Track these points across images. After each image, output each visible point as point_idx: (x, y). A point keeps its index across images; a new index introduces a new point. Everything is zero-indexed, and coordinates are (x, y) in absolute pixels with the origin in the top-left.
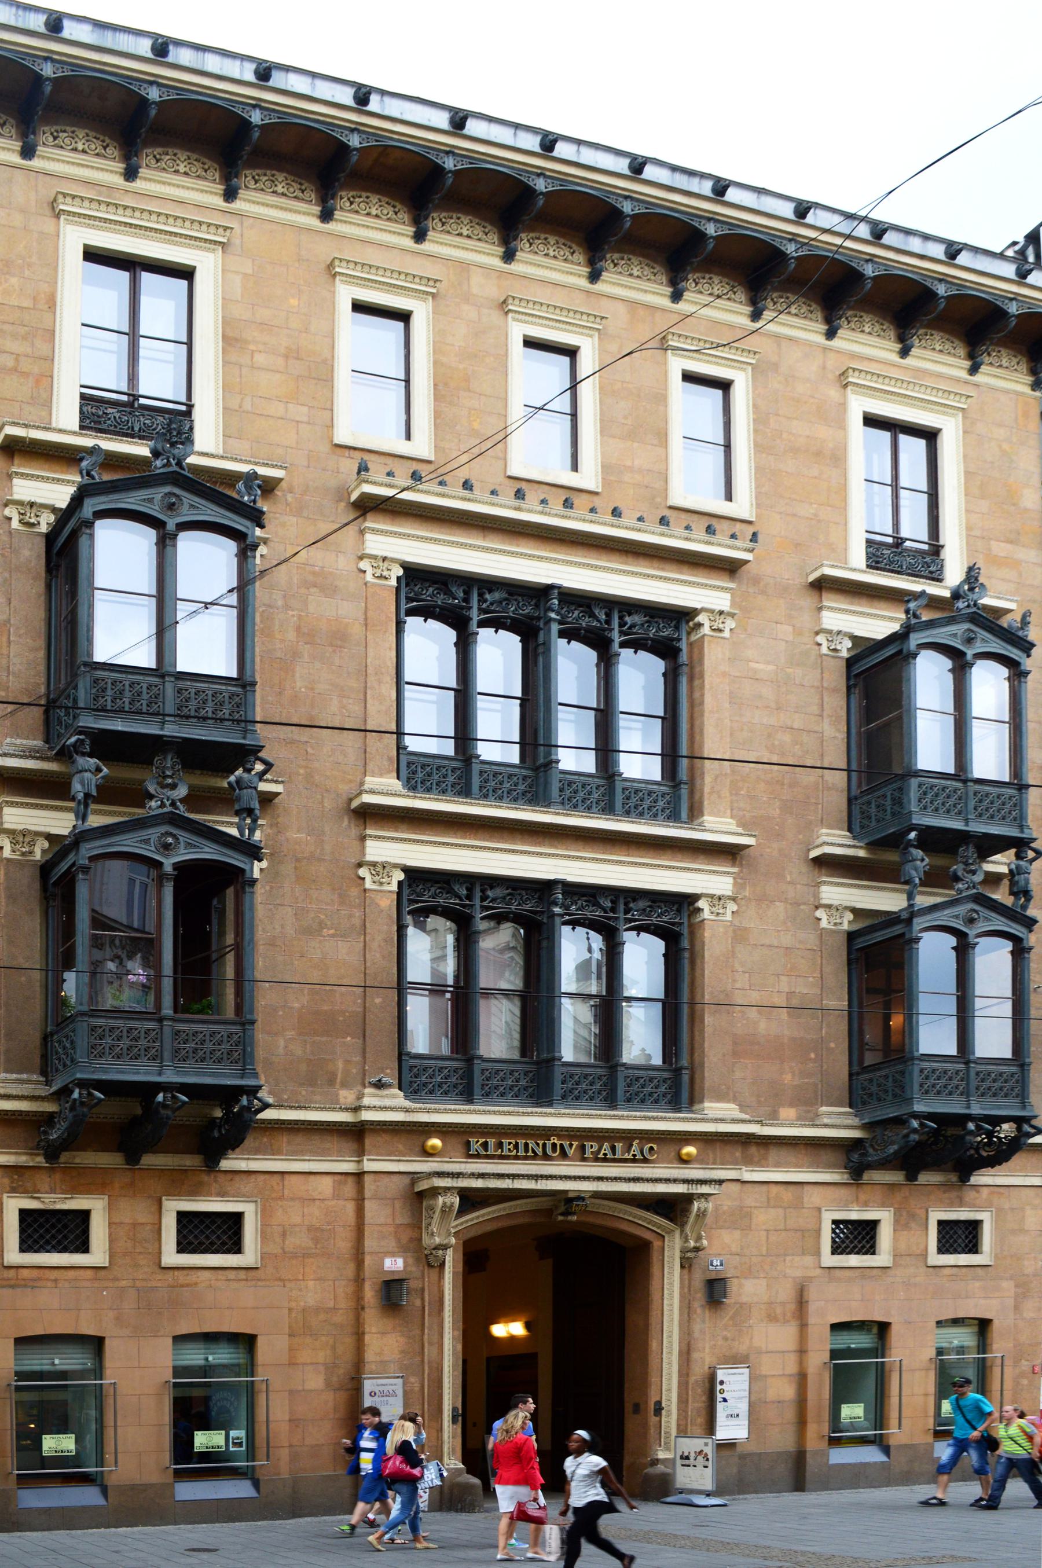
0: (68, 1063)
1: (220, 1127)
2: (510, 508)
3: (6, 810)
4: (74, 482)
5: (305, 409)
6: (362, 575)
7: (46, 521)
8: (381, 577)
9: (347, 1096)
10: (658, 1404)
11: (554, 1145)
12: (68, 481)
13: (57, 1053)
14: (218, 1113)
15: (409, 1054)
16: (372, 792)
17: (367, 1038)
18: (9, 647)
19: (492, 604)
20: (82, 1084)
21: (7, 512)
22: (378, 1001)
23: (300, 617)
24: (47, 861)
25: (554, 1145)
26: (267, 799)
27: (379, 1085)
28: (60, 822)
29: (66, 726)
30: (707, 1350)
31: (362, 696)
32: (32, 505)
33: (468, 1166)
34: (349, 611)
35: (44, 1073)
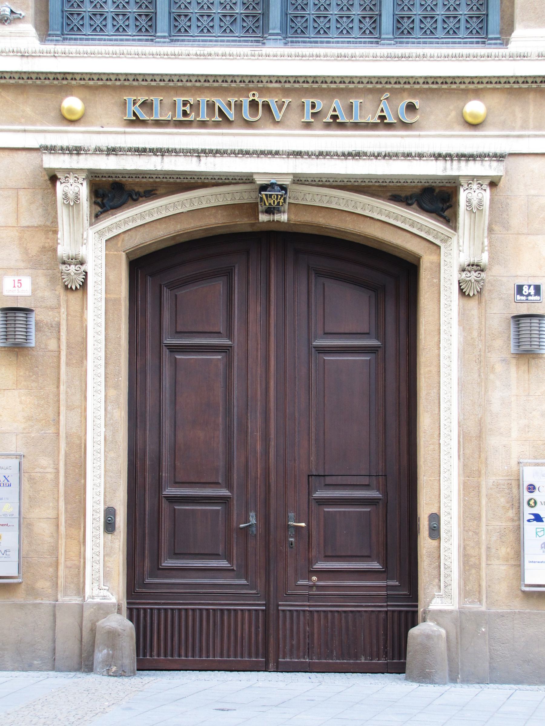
10: (435, 518)
11: (254, 104)
25: (254, 104)
30: (514, 434)
33: (128, 137)
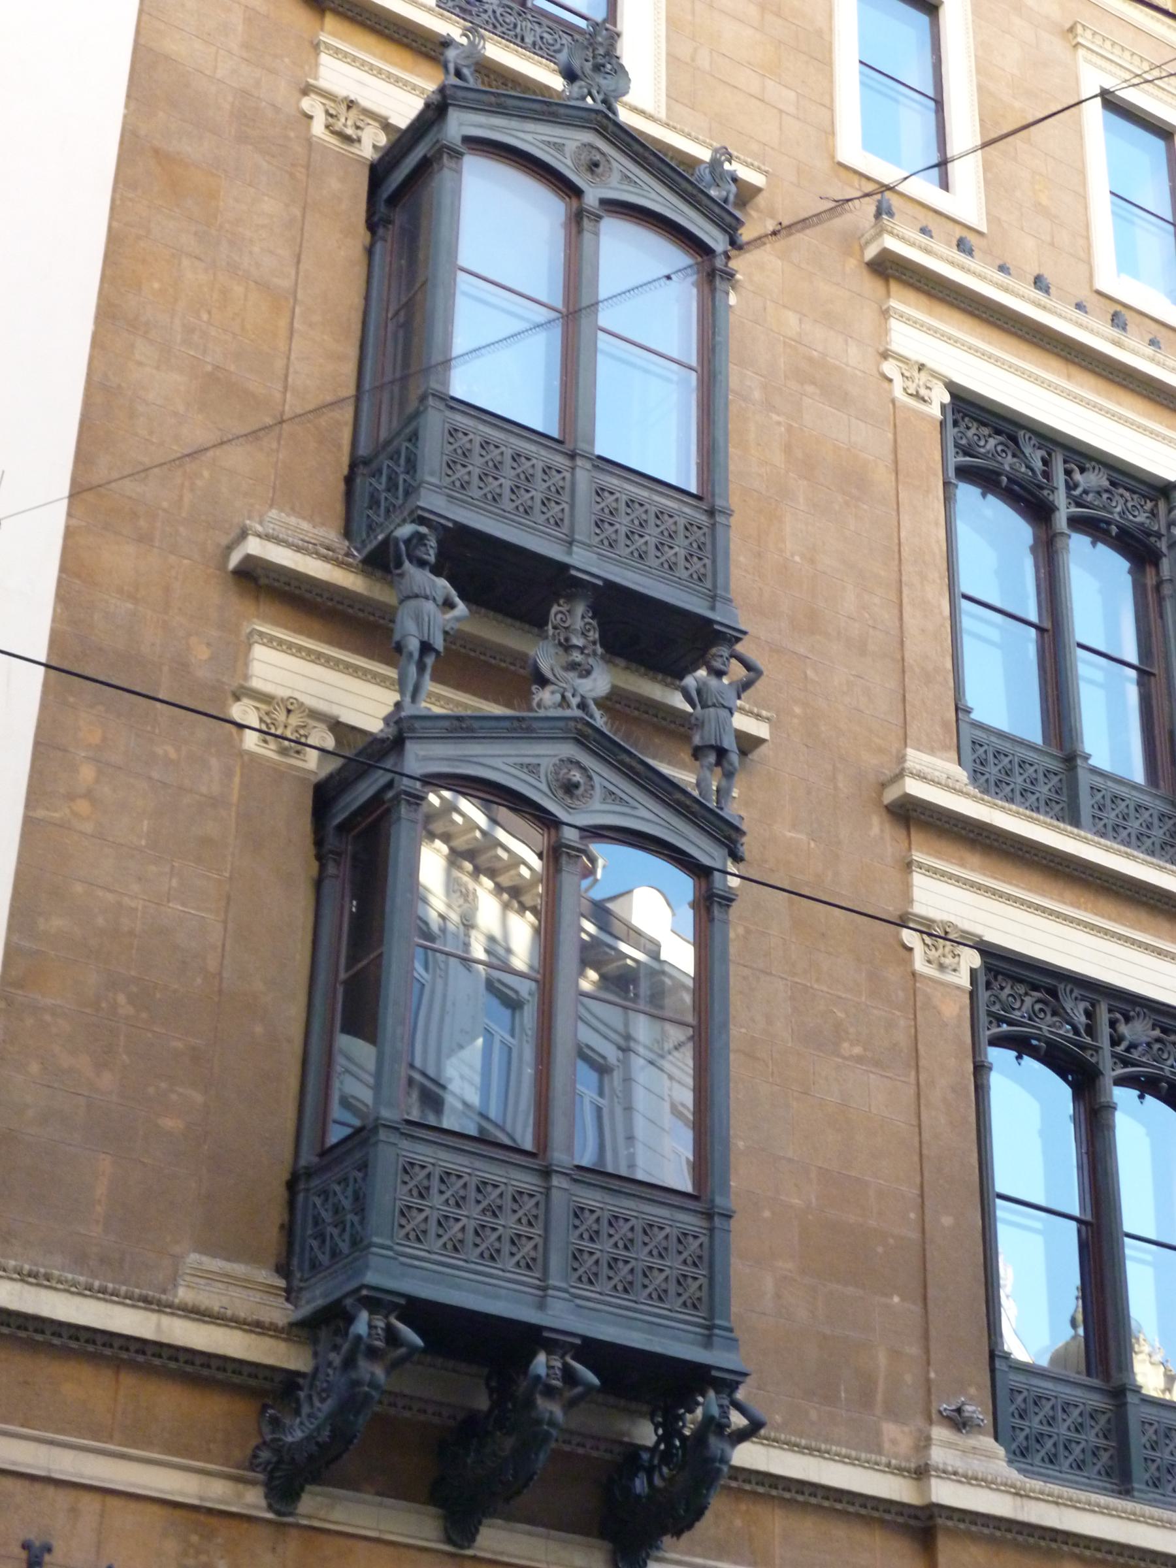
0: (344, 1247)
1: (650, 1471)
2: (1106, 339)
3: (260, 652)
4: (423, 91)
5: (792, 95)
6: (886, 384)
7: (372, 142)
8: (917, 396)
9: (897, 1437)
12: (414, 87)
13: (317, 1221)
14: (646, 1434)
15: (1007, 1357)
16: (922, 777)
17: (931, 1305)
18: (291, 338)
19: (1086, 492)
20: (375, 1302)
21: (307, 104)
22: (947, 1221)
23: (790, 428)
24: (331, 776)
26: (748, 744)
27: (959, 1422)
28: (367, 703)
29: (388, 511)
31: (893, 596)
32: (351, 104)
34: (869, 442)
35: (283, 1270)
